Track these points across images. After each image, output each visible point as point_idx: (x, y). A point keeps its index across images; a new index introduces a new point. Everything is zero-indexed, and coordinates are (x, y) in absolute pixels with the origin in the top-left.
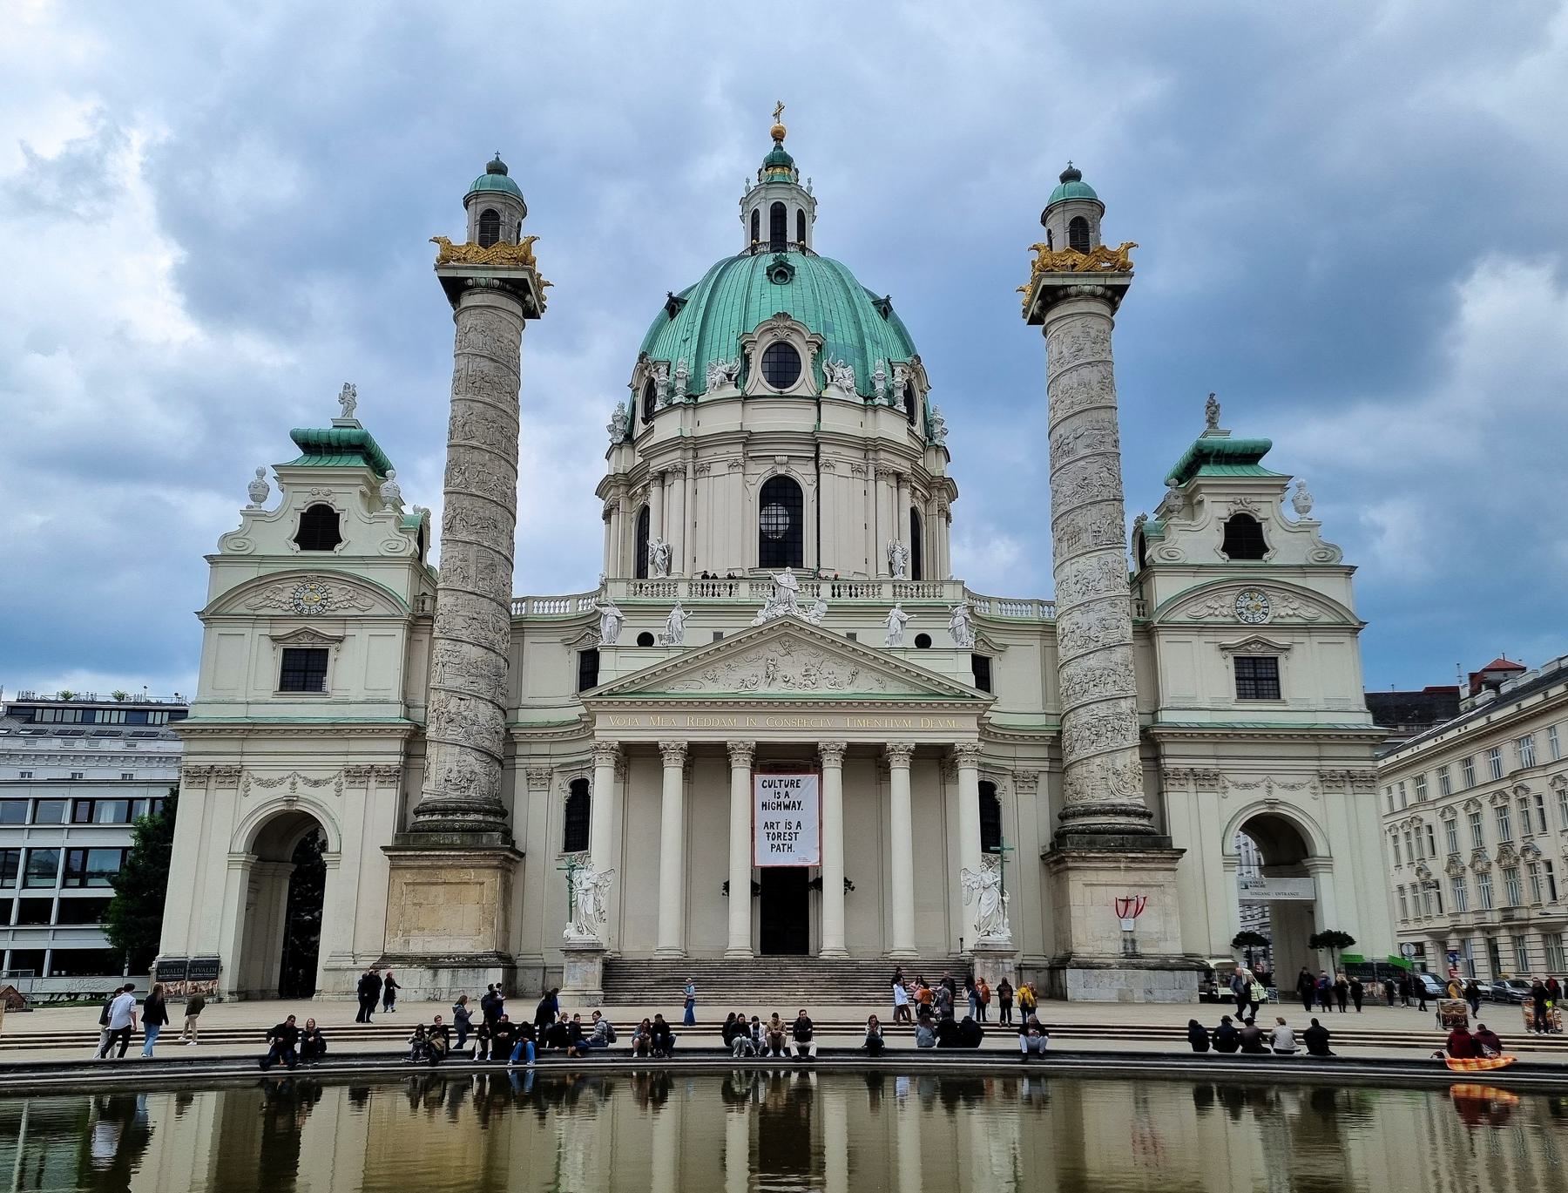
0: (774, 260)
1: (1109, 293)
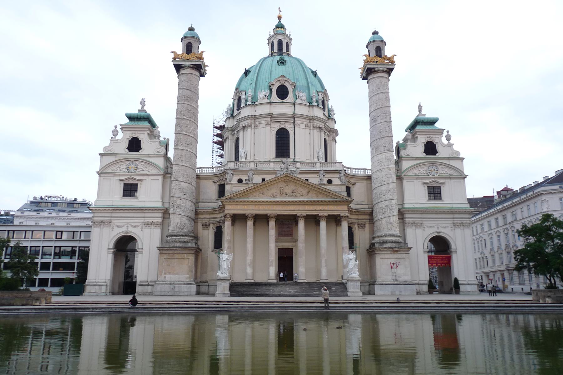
0: (280, 58)
1: (388, 70)
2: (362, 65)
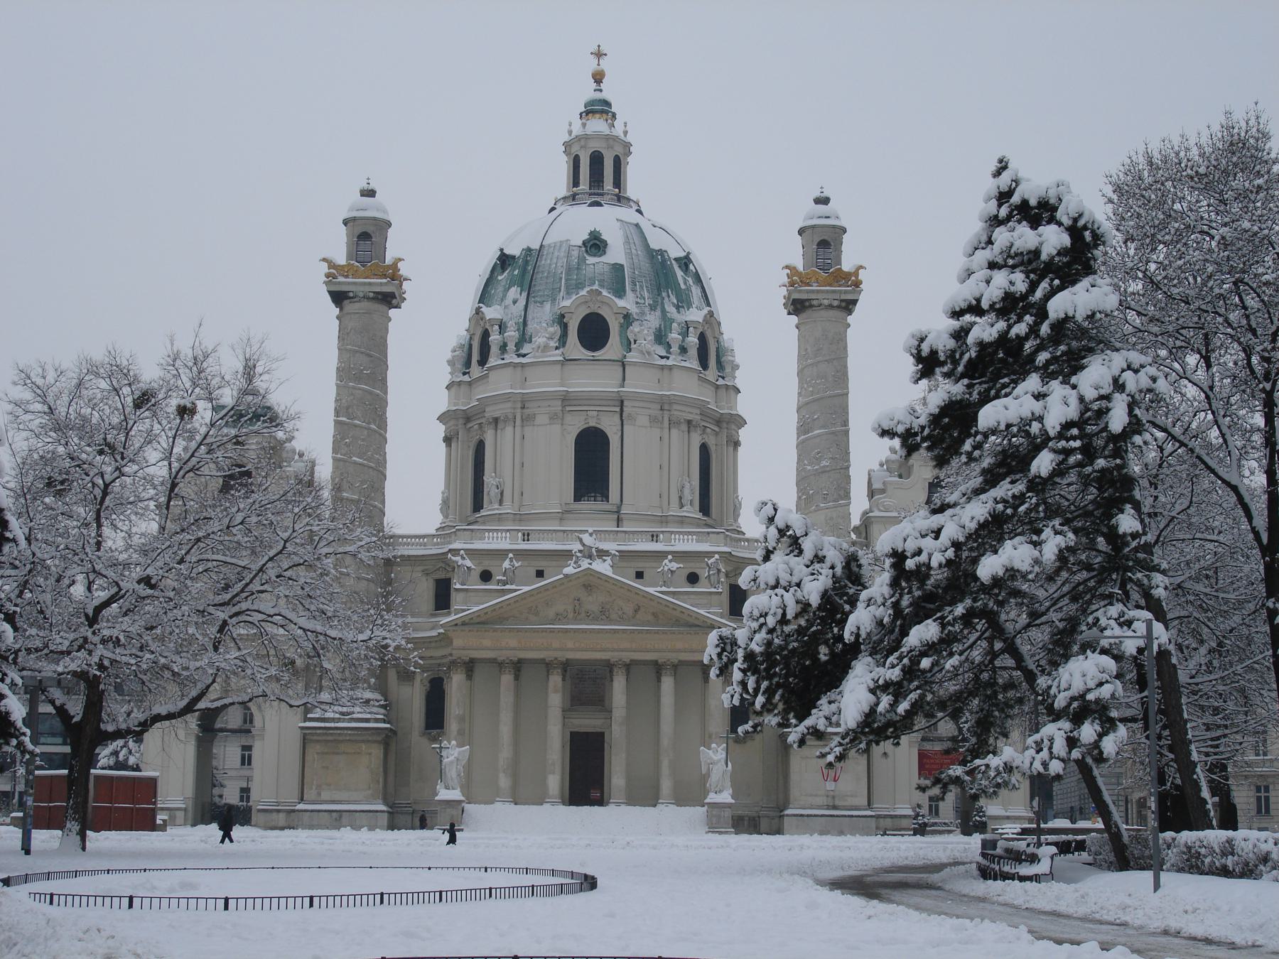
2: (786, 280)
